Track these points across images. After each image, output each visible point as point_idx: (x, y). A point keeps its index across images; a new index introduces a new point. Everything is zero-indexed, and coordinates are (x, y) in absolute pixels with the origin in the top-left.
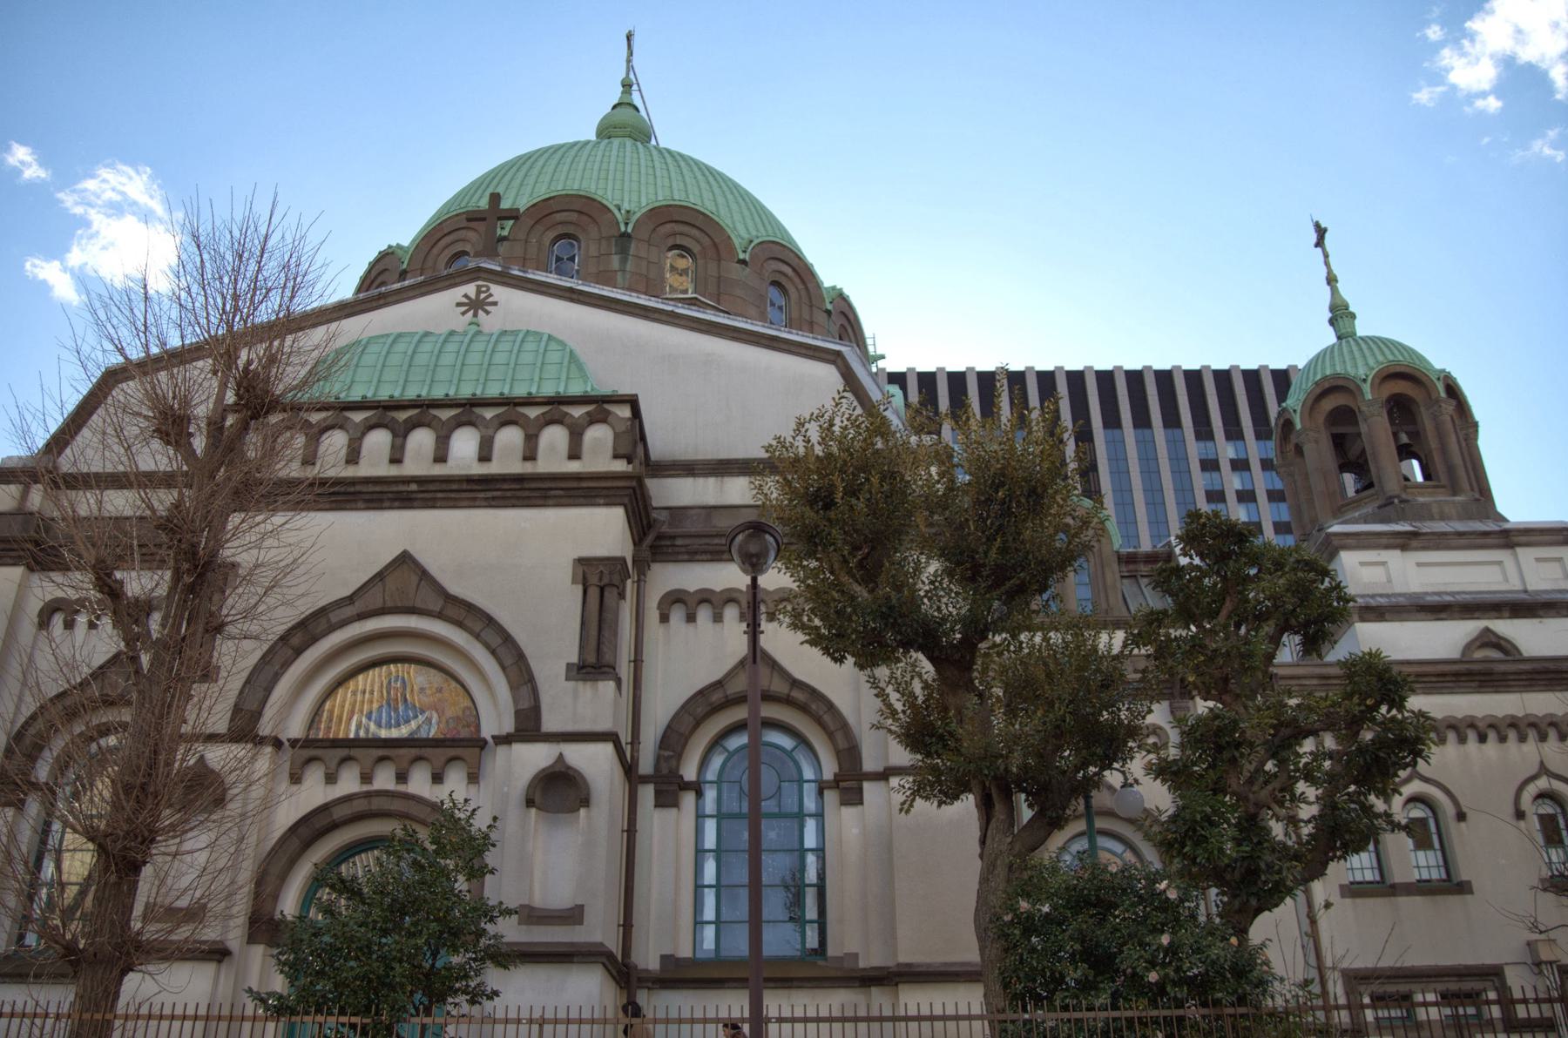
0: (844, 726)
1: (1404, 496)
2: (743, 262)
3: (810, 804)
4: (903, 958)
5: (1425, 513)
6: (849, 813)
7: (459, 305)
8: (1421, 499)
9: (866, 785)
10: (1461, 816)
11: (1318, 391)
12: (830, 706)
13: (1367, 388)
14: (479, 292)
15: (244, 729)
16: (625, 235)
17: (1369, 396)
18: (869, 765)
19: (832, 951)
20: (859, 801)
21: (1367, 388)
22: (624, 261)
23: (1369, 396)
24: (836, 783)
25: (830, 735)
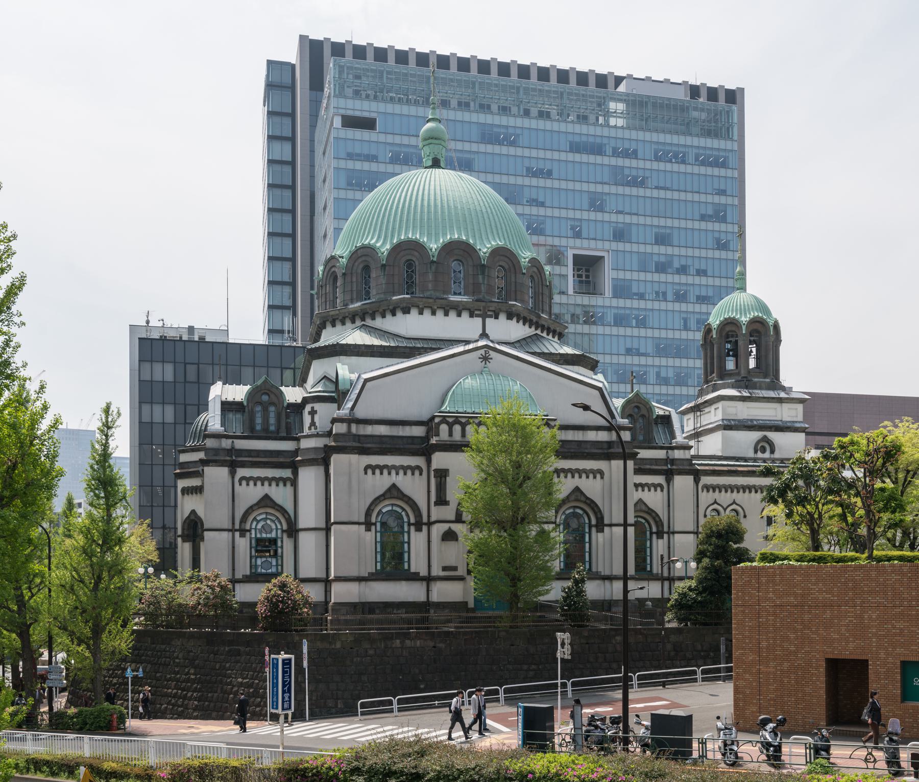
0: (600, 511)
1: (749, 378)
2: (524, 274)
3: (587, 530)
4: (614, 574)
5: (754, 386)
6: (600, 535)
7: (480, 358)
8: (756, 380)
9: (605, 528)
10: (745, 516)
11: (726, 322)
12: (597, 505)
13: (744, 328)
14: (486, 354)
15: (459, 519)
16: (483, 265)
17: (744, 332)
18: (606, 521)
19: (594, 570)
20: (603, 532)
21: (744, 328)
22: (484, 278)
23: (744, 332)
24: (596, 526)
25: (595, 513)
